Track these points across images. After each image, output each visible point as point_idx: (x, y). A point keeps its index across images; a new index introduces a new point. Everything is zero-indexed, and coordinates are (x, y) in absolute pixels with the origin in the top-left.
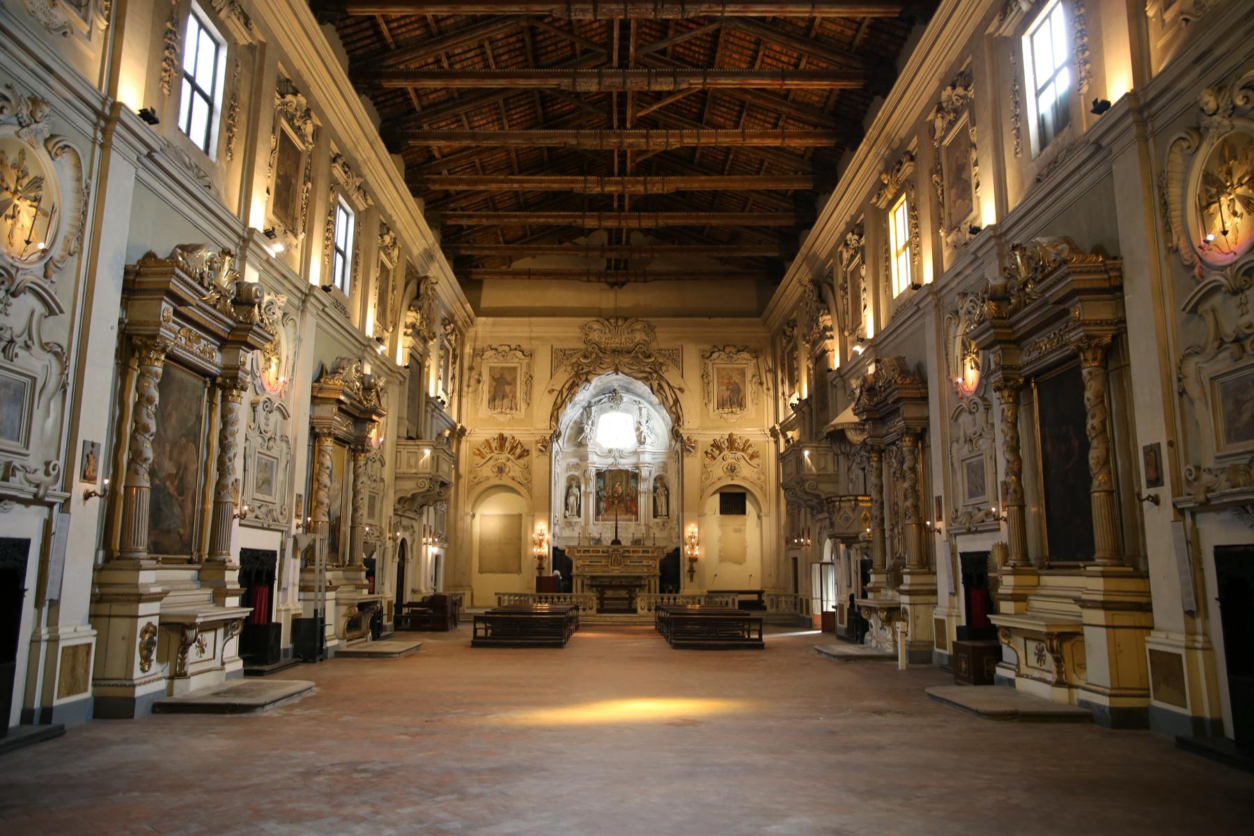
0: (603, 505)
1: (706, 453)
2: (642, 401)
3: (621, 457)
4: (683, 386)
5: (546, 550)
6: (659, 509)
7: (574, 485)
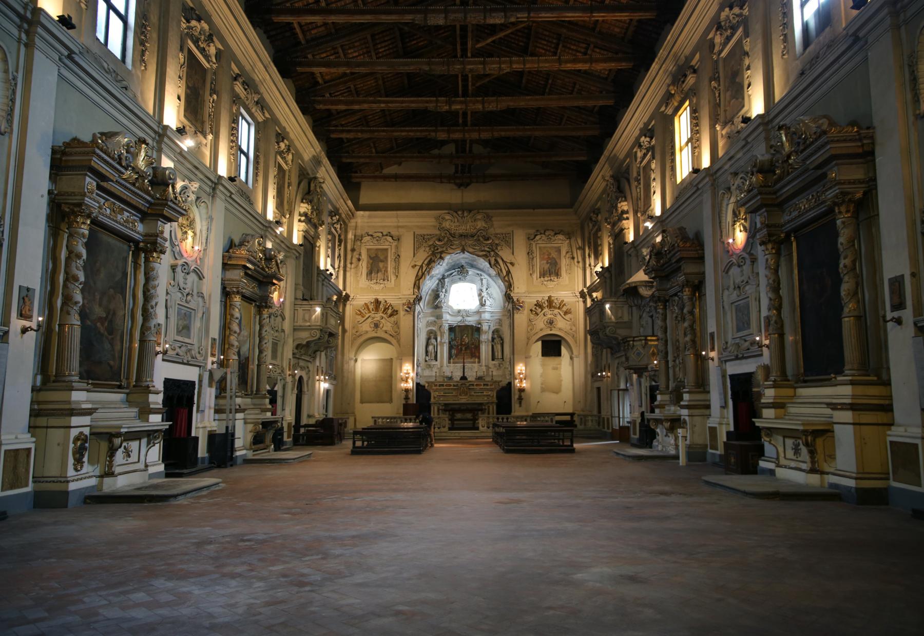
3: (467, 316)
4: (513, 261)
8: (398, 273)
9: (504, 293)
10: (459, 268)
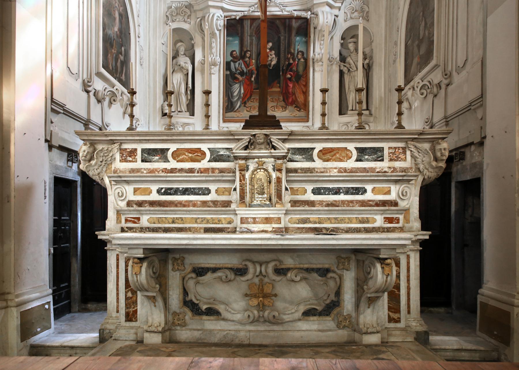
0: (237, 89)
7: (182, 50)
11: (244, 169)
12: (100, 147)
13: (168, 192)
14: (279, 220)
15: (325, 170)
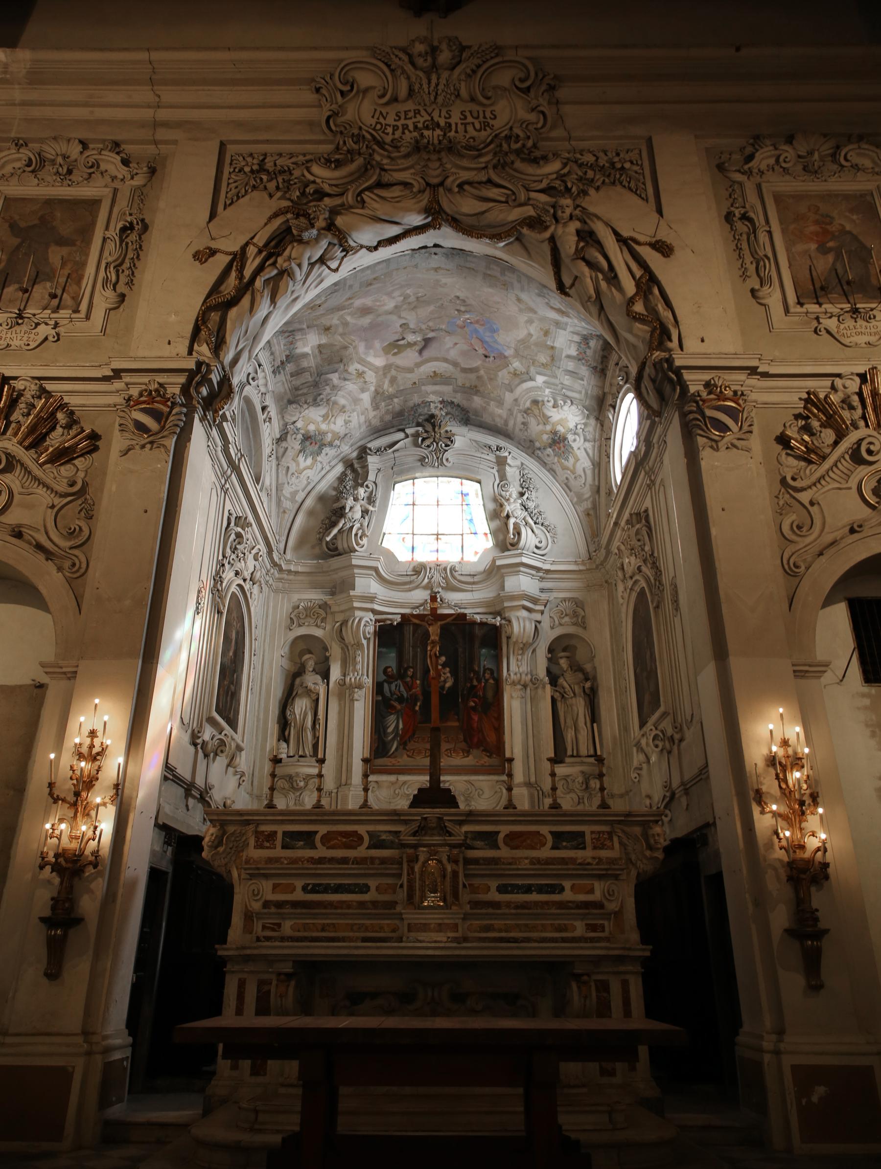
0: (393, 723)
1: (783, 441)
2: (502, 443)
3: (450, 588)
4: (664, 235)
5: (106, 826)
6: (569, 735)
7: (310, 665)
8: (130, 283)
9: (588, 505)
10: (418, 425)
11: (413, 859)
12: (231, 829)
13: (316, 889)
14: (455, 927)
15: (514, 861)
